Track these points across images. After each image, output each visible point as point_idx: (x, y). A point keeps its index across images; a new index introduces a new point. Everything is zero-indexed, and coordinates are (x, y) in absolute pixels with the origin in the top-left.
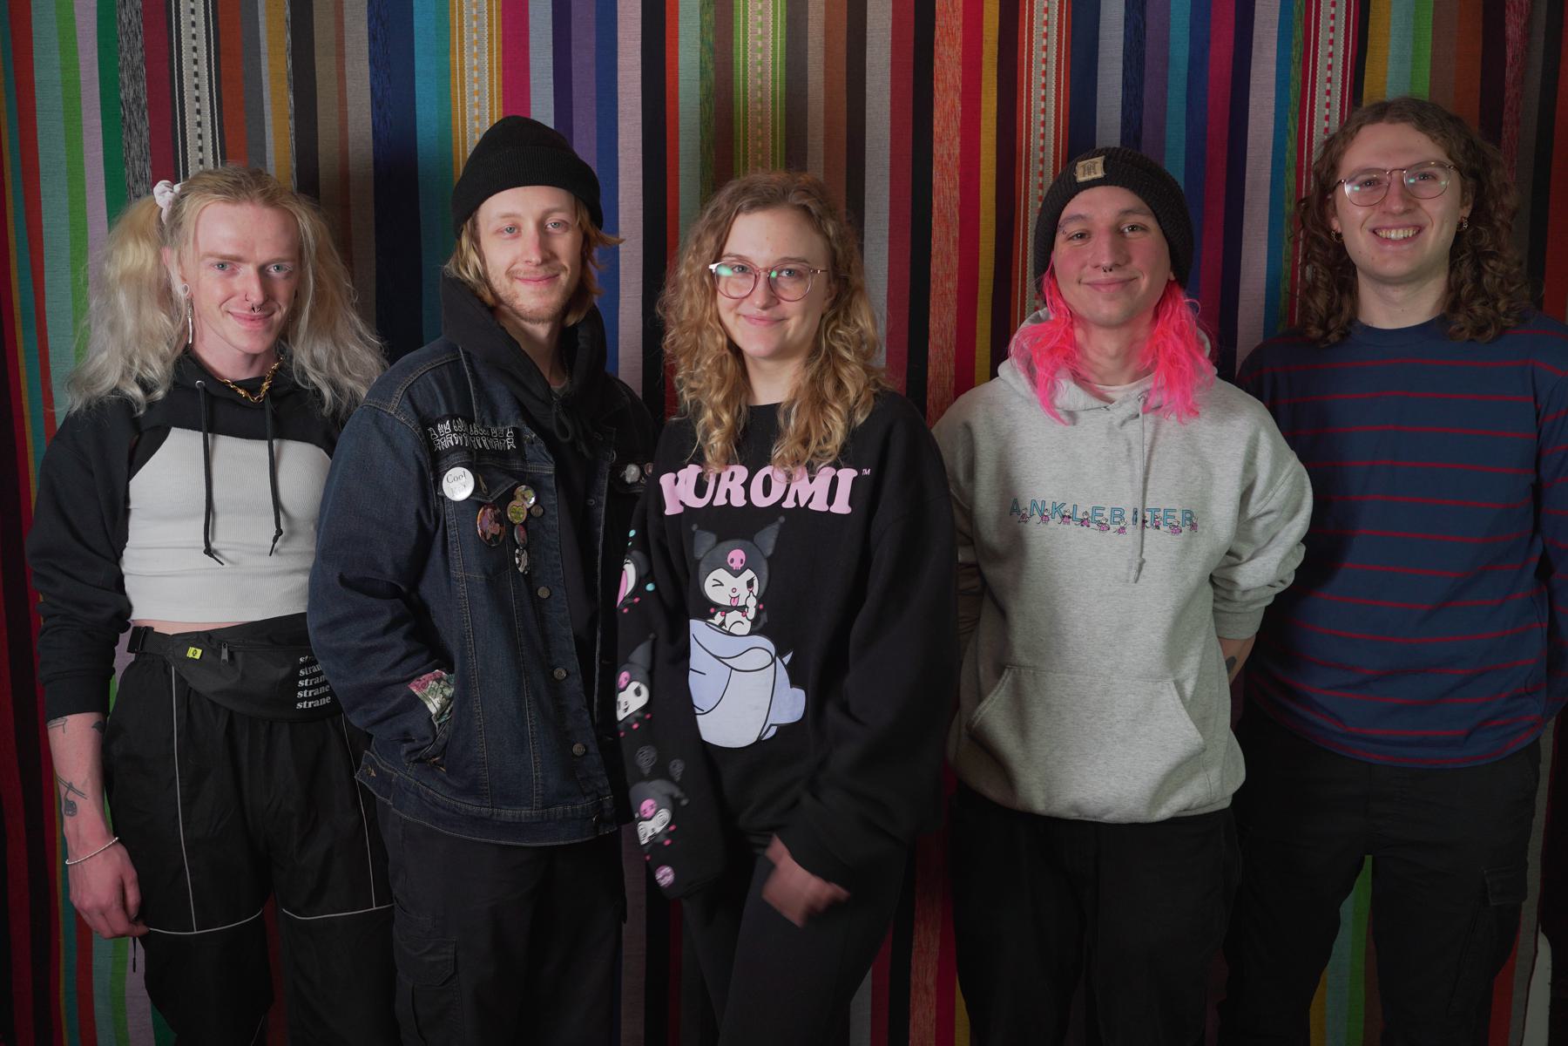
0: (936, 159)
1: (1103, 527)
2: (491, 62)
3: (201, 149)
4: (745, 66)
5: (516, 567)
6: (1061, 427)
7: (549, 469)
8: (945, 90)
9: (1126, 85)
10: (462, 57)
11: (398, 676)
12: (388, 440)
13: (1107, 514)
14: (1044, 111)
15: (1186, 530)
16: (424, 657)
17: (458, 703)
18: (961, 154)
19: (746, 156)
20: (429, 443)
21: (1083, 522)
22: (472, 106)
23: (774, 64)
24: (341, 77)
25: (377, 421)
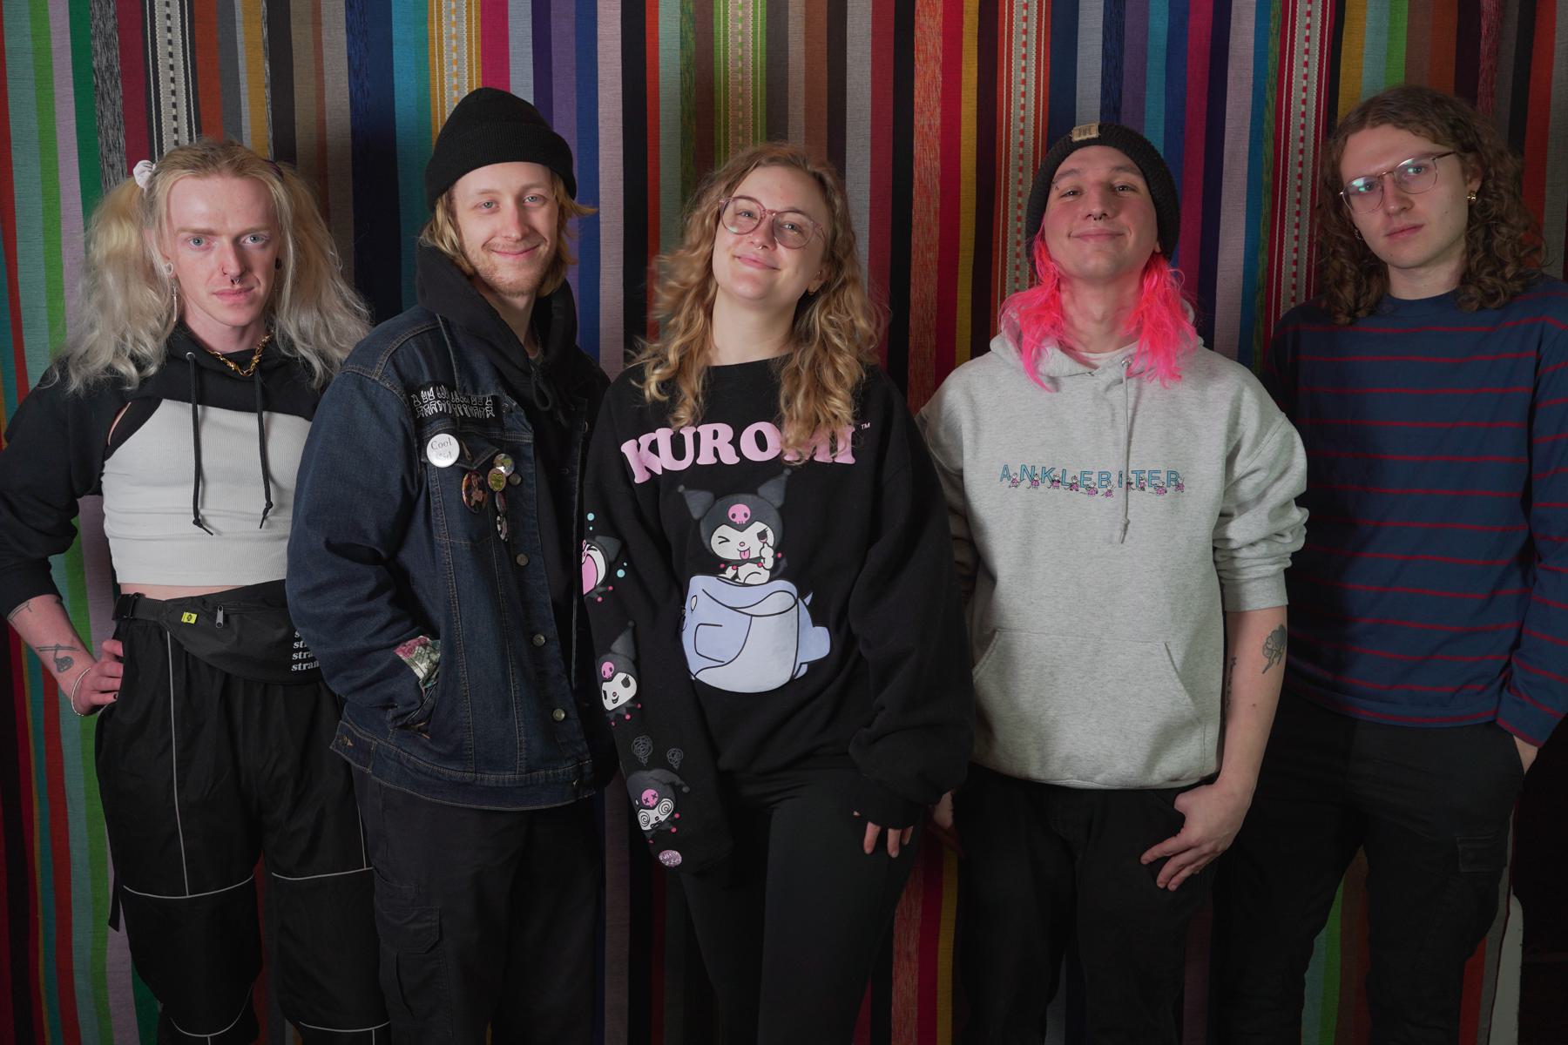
1: (1091, 491)
3: (175, 118)
4: (726, 35)
5: (498, 534)
6: (1046, 394)
7: (527, 438)
8: (925, 61)
9: (1106, 56)
10: (440, 26)
11: (385, 642)
12: (373, 406)
13: (1095, 478)
14: (1024, 82)
15: (1171, 490)
16: (408, 623)
17: (444, 670)
18: (942, 124)
19: (726, 126)
20: (413, 410)
21: (1072, 486)
23: (755, 34)
24: (318, 45)
25: (361, 387)
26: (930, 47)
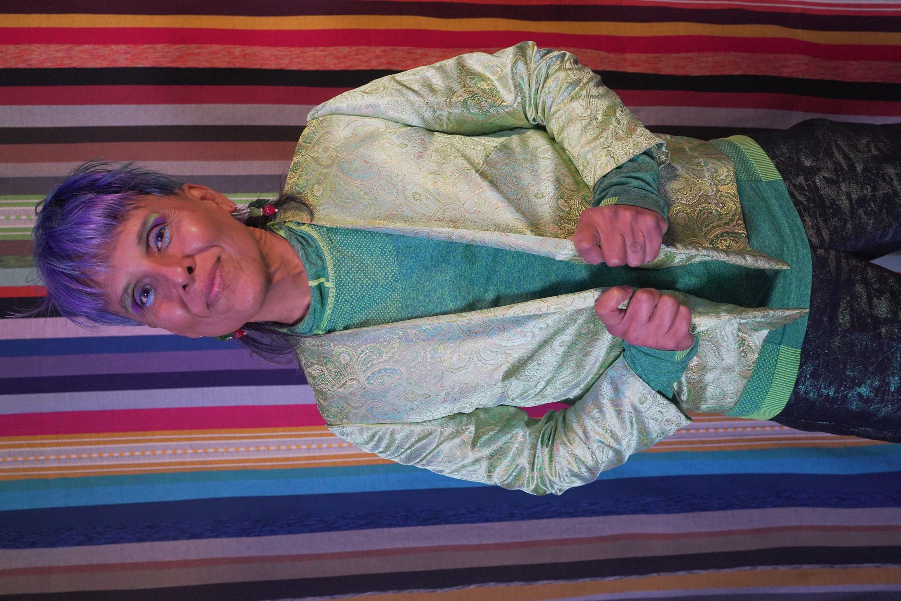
8: (70, 58)
18: (125, 43)
22: (90, 458)
24: (68, 570)
26: (58, 54)
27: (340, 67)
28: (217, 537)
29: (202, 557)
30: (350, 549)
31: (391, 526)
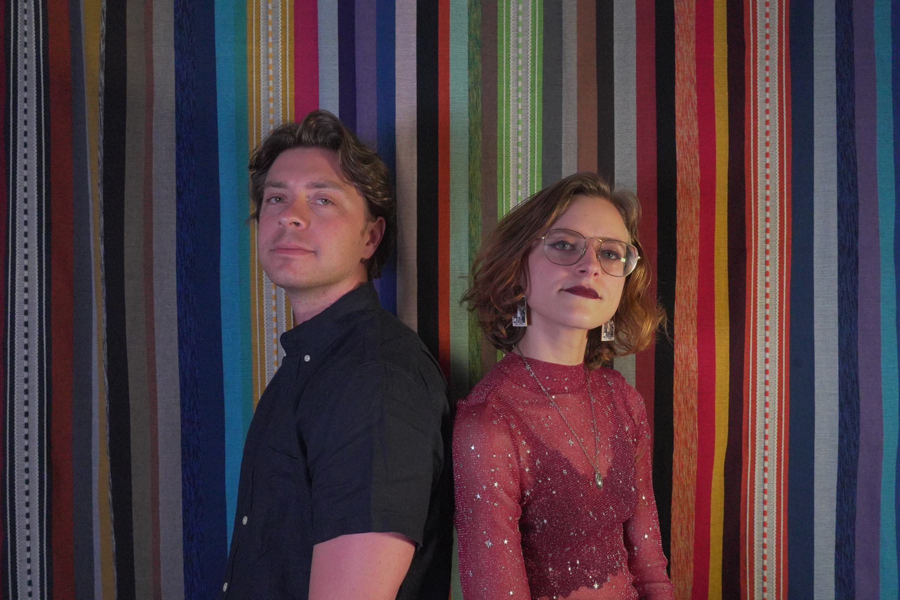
0: (678, 140)
2: (284, 50)
4: (508, 59)
8: (683, 81)
10: (258, 46)
18: (700, 135)
19: (508, 138)
23: (533, 57)
24: (149, 61)
27: (677, 361)
28: (178, 218)
29: (155, 201)
30: (158, 360)
31: (183, 405)
